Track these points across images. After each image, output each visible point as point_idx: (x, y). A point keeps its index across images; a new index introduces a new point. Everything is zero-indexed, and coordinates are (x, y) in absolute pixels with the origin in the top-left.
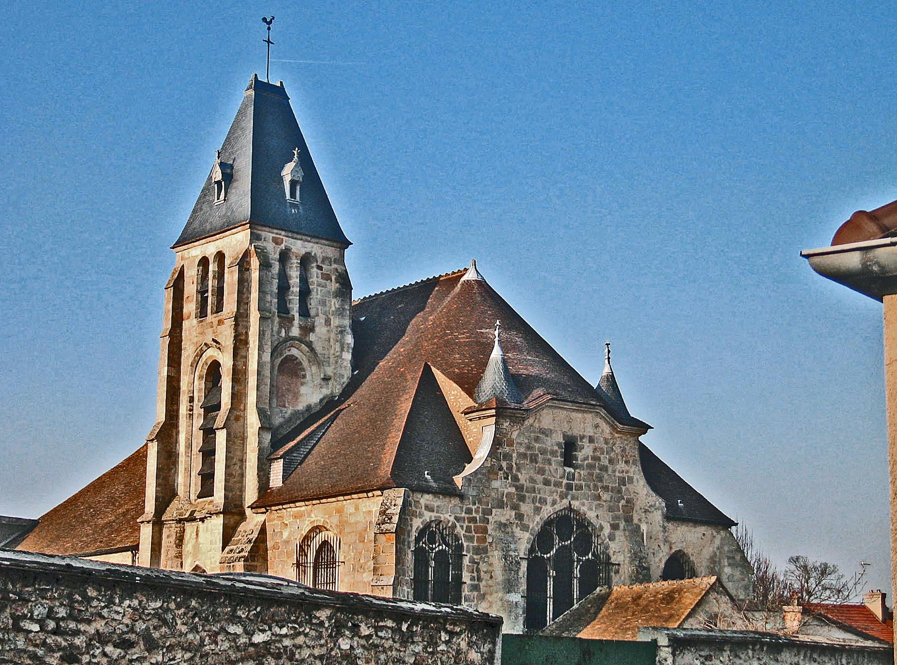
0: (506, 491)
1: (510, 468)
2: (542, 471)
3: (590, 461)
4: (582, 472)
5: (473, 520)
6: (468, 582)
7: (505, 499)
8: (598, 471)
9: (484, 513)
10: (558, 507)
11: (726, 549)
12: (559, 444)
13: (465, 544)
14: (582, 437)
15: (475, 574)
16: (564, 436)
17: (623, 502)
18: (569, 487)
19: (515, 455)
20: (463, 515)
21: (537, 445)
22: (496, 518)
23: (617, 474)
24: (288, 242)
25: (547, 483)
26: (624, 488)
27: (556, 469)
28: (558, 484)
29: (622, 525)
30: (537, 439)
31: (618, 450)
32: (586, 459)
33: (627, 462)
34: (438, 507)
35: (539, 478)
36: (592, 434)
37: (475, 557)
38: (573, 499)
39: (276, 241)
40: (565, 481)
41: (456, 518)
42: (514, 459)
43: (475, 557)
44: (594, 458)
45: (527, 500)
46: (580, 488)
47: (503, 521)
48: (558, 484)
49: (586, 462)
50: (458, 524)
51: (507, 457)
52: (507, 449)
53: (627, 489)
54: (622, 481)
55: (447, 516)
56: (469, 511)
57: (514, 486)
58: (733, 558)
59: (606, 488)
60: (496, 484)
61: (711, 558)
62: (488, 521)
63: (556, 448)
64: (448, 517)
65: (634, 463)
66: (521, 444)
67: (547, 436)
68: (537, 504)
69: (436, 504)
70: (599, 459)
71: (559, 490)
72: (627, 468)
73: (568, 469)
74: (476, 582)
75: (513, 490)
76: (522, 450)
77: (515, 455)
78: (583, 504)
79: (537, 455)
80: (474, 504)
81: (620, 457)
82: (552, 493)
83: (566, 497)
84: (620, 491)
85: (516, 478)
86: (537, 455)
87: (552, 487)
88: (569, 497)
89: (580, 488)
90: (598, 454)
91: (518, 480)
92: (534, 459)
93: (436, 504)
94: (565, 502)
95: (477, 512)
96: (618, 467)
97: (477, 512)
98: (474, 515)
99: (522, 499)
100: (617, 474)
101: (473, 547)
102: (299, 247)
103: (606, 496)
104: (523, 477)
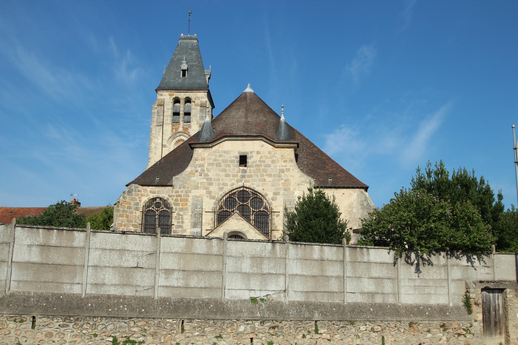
0: (200, 181)
1: (203, 171)
2: (224, 170)
3: (258, 163)
4: (252, 169)
5: (180, 196)
6: (176, 224)
7: (199, 185)
8: (263, 167)
9: (186, 192)
10: (235, 187)
11: (360, 200)
12: (236, 157)
13: (174, 207)
14: (251, 152)
15: (180, 220)
16: (239, 152)
17: (283, 181)
18: (243, 177)
19: (206, 165)
20: (174, 194)
21: (220, 159)
22: (194, 194)
23: (278, 168)
24: (176, 94)
25: (227, 175)
26: (282, 174)
27: (236, 168)
28: (233, 176)
29: (282, 192)
30: (220, 156)
31: (279, 156)
32: (254, 162)
33: (284, 161)
34: (158, 191)
35: (223, 174)
37: (180, 212)
38: (246, 181)
39: (171, 95)
40: (240, 174)
41: (169, 196)
42: (206, 166)
43: (180, 212)
44: (260, 161)
45: (214, 184)
46: (251, 176)
47: (198, 195)
48: (233, 176)
50: (170, 199)
51: (200, 166)
52: (201, 162)
53: (286, 175)
54: (282, 171)
55: (164, 195)
56: (177, 192)
57: (205, 178)
58: (363, 205)
59: (270, 176)
60: (193, 179)
61: (350, 206)
62: (188, 196)
63: (234, 159)
64: (165, 196)
65: (291, 161)
66: (210, 159)
67: (227, 154)
68: (221, 186)
69: (156, 190)
70: (264, 161)
71: (236, 178)
72: (285, 164)
73: (242, 168)
74: (181, 224)
75: (205, 180)
77: (206, 165)
78: (253, 184)
79: (221, 163)
80: (180, 188)
82: (231, 180)
83: (241, 181)
84: (280, 176)
85: (207, 175)
86: (221, 163)
87: (231, 177)
88: (243, 181)
89: (251, 176)
91: (208, 176)
93: (156, 190)
94: (241, 184)
95: (182, 192)
96: (279, 164)
97: (182, 192)
98: (180, 193)
99: (211, 184)
100: (278, 168)
101: (179, 208)
102: (182, 96)
103: (268, 179)
104: (211, 175)
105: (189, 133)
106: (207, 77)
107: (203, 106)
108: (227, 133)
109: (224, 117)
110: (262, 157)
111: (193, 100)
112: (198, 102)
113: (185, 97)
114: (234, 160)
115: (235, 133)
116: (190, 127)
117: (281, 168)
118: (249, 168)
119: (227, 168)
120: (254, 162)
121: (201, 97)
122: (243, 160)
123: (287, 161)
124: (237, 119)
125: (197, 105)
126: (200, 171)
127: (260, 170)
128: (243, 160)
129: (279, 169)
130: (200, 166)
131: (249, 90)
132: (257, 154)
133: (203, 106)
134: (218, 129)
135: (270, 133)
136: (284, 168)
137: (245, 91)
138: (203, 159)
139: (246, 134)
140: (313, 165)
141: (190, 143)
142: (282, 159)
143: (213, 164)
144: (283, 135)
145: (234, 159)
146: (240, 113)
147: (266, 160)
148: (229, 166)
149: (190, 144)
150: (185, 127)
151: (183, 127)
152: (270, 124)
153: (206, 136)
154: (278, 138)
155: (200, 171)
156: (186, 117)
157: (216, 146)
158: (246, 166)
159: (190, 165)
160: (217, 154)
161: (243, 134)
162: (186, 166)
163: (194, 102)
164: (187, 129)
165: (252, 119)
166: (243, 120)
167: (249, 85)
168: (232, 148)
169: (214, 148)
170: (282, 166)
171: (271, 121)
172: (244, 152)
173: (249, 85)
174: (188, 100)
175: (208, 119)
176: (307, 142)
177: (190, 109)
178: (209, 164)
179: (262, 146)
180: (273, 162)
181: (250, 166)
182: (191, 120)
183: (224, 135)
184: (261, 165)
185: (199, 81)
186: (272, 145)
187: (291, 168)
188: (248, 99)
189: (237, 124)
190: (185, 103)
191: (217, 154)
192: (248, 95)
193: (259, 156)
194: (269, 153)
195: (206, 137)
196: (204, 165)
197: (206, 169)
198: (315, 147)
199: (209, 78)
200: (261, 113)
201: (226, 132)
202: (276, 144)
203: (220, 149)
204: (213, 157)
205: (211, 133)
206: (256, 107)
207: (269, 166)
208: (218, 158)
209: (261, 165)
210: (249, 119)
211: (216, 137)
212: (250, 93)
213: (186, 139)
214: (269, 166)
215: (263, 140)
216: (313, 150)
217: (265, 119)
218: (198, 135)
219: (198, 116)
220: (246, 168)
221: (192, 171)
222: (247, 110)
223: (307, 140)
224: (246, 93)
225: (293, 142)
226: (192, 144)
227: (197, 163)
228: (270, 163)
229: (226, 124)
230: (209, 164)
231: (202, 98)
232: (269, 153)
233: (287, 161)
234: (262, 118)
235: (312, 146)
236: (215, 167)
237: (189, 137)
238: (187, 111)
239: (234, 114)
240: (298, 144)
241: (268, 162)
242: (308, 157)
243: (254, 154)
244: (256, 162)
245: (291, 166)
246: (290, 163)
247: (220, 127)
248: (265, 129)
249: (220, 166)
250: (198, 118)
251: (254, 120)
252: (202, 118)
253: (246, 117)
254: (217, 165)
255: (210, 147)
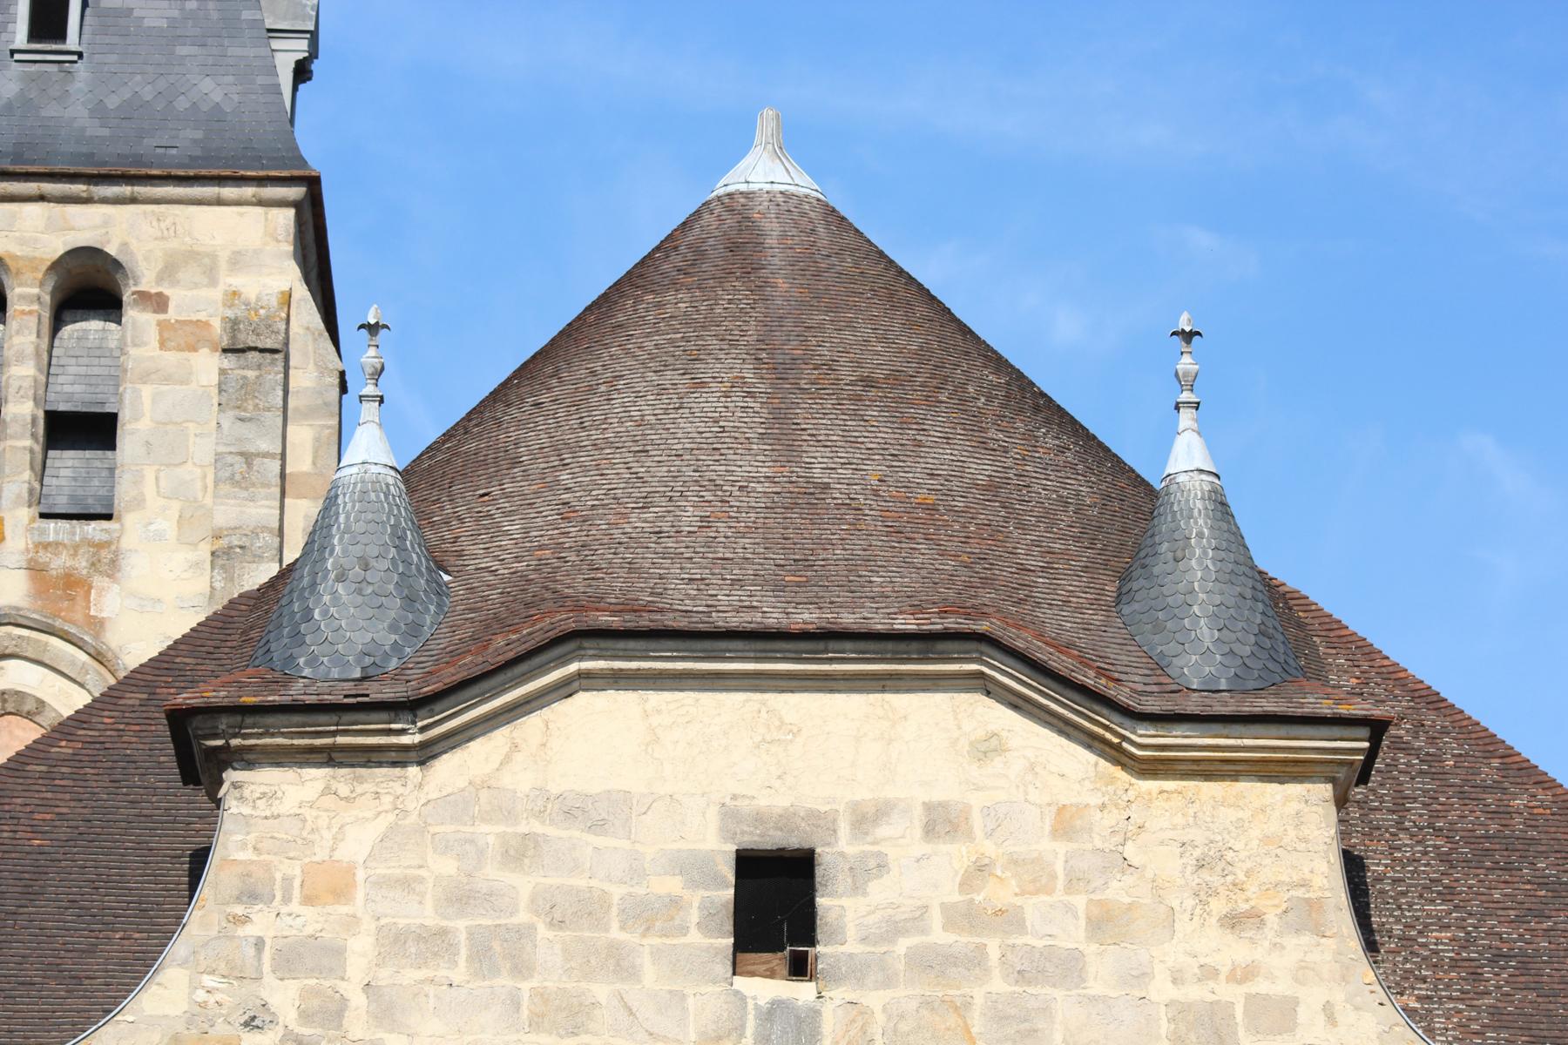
3: (939, 935)
4: (874, 1000)
8: (999, 985)
12: (692, 868)
14: (866, 819)
16: (729, 815)
19: (360, 949)
21: (523, 884)
23: (1161, 990)
30: (521, 852)
31: (1168, 864)
32: (895, 929)
33: (1233, 922)
36: (946, 790)
44: (965, 917)
49: (903, 945)
51: (290, 960)
52: (307, 920)
63: (673, 885)
65: (1305, 916)
66: (407, 884)
67: (598, 826)
72: (1234, 951)
76: (423, 913)
79: (524, 933)
81: (1181, 900)
86: (524, 933)
90: (999, 893)
92: (501, 952)
100: (1161, 990)
105: (97, 625)
106: (289, 53)
107: (250, 345)
108: (597, 602)
109: (530, 433)
110: (981, 868)
111: (148, 283)
112: (197, 301)
113: (56, 246)
114: (675, 903)
115: (684, 603)
116: (108, 562)
117: (1194, 993)
118: (838, 994)
119: (601, 991)
120: (895, 929)
121: (230, 250)
122: (775, 901)
123: (1255, 917)
124: (685, 465)
125: (186, 336)
126: (289, 1016)
127: (961, 1008)
128: (775, 901)
129: (1180, 1010)
130: (290, 960)
131: (763, 172)
132: (930, 831)
133: (250, 345)
134: (477, 556)
135: (1064, 616)
136: (1233, 994)
137: (734, 181)
138: (331, 885)
139: (806, 617)
140: (1525, 964)
141: (186, 698)
142: (1204, 894)
143: (435, 943)
144: (1206, 633)
145: (673, 885)
146: (709, 401)
147: (1032, 908)
148: (620, 964)
149: (179, 719)
150: (59, 563)
151: (35, 569)
152: (1048, 518)
153: (349, 633)
154: (1159, 667)
155: (289, 1016)
156: (68, 462)
157: (476, 746)
158: (800, 968)
159: (179, 947)
160: (489, 833)
161: (774, 618)
162: (138, 965)
163: (158, 303)
164: (72, 586)
165: (852, 456)
166: (753, 467)
167: (767, 121)
168: (649, 771)
169: (448, 767)
170: (1209, 973)
171: (1044, 488)
172: (786, 820)
173: (767, 121)
174: (89, 289)
175: (373, 451)
176: (1430, 718)
177: (116, 381)
178: (395, 942)
179: (988, 748)
180: (1103, 923)
181: (857, 972)
182: (124, 492)
183: (567, 621)
184: (975, 961)
185: (212, 90)
186: (1092, 742)
187: (1311, 999)
188: (775, 258)
189: (689, 516)
190: (57, 323)
191: (489, 833)
192: (772, 229)
193: (954, 856)
194: (1065, 823)
195: (361, 639)
196: (339, 952)
197: (358, 999)
198: (1523, 772)
199: (302, 72)
200: (931, 402)
201: (578, 585)
202: (1144, 737)
203: (520, 780)
204: (446, 866)
205: (410, 600)
206: (868, 342)
207: (1069, 968)
208: (493, 874)
209: (975, 961)
210: (818, 463)
211: (480, 641)
212: (788, 203)
213: (67, 700)
214: (1069, 968)
215: (982, 684)
216: (1503, 813)
217: (981, 469)
218: (250, 623)
219: (202, 448)
220: (803, 991)
221: (199, 1015)
222: (780, 371)
223: (1435, 701)
224: (737, 207)
225: (1326, 708)
226: (194, 711)
227: (262, 923)
228: (1073, 936)
229: (567, 512)
230: (395, 942)
231: (238, 261)
232: (1065, 823)
233: (1255, 917)
234: (948, 459)
235: (1489, 772)
236: (459, 973)
237: (100, 681)
238: (72, 395)
239: (647, 408)
240: (1377, 728)
241: (1055, 923)
242: (1467, 882)
243: (900, 839)
244: (917, 921)
245: (1302, 972)
246: (1299, 946)
247: (504, 541)
248: (1005, 573)
249: (521, 969)
250: (197, 469)
251: (874, 471)
252: (237, 470)
253: (783, 435)
254: (482, 957)
255: (401, 757)
